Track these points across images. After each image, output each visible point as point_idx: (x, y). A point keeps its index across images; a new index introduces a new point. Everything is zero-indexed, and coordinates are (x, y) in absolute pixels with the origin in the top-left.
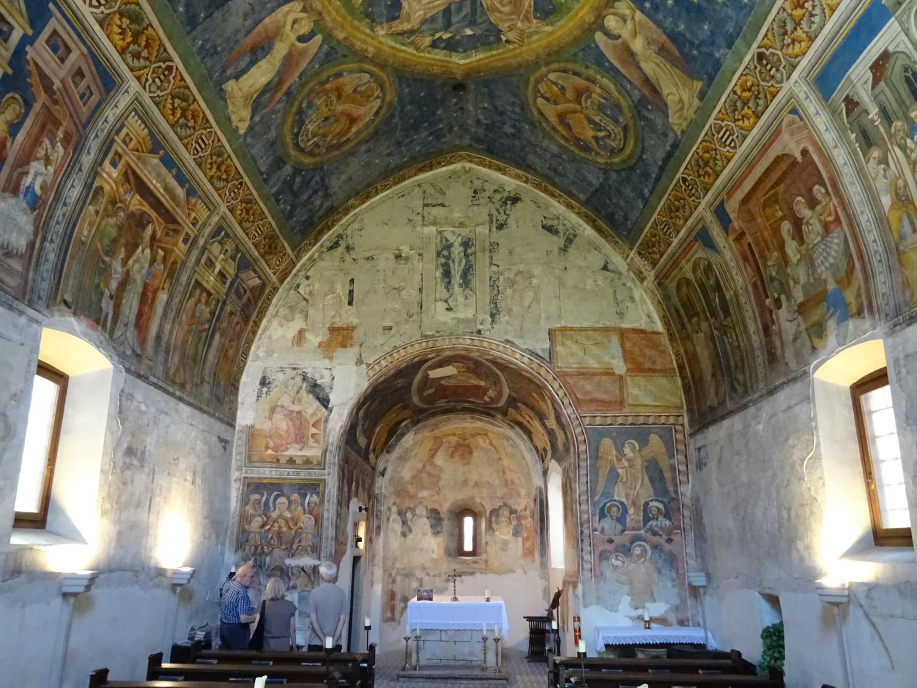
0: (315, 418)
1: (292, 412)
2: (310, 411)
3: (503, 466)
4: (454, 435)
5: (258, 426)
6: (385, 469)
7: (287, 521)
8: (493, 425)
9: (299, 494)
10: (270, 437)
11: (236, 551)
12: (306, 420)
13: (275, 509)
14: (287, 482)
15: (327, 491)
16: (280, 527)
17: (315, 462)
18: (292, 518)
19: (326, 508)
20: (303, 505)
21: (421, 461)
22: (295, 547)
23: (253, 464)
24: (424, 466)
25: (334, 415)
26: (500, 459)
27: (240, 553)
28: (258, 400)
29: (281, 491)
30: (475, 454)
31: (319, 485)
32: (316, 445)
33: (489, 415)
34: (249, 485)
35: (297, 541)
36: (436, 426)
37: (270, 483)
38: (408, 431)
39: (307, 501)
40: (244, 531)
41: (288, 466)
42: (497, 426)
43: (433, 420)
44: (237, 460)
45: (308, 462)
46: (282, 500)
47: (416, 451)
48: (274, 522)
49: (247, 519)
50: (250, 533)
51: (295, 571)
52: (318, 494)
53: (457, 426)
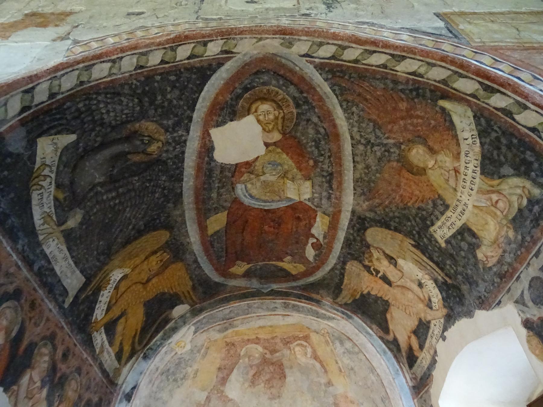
3: (335, 397)
4: (257, 341)
6: (134, 388)
8: (317, 315)
21: (203, 389)
24: (208, 399)
26: (329, 383)
30: (290, 379)
33: (310, 299)
36: (228, 322)
38: (185, 323)
42: (324, 317)
43: (224, 310)
47: (195, 367)
53: (261, 323)
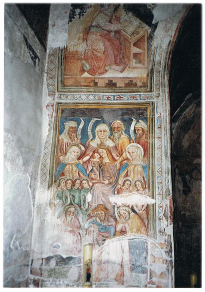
0: (137, 37)
1: (109, 32)
2: (131, 29)
5: (71, 49)
7: (109, 152)
9: (123, 120)
10: (86, 59)
11: (50, 186)
12: (126, 39)
13: (94, 137)
14: (107, 107)
15: (157, 116)
16: (101, 157)
17: (139, 84)
18: (116, 147)
19: (157, 135)
20: (127, 131)
22: (121, 182)
23: (67, 89)
25: (159, 32)
27: (54, 189)
28: (70, 21)
29: (102, 117)
31: (146, 110)
32: (140, 65)
34: (63, 111)
35: (123, 174)
37: (87, 109)
39: (132, 128)
40: (58, 163)
41: (107, 89)
44: (48, 85)
45: (130, 84)
46: (102, 127)
48: (94, 152)
49: (62, 149)
50: (66, 165)
51: (122, 212)
52: (145, 119)
